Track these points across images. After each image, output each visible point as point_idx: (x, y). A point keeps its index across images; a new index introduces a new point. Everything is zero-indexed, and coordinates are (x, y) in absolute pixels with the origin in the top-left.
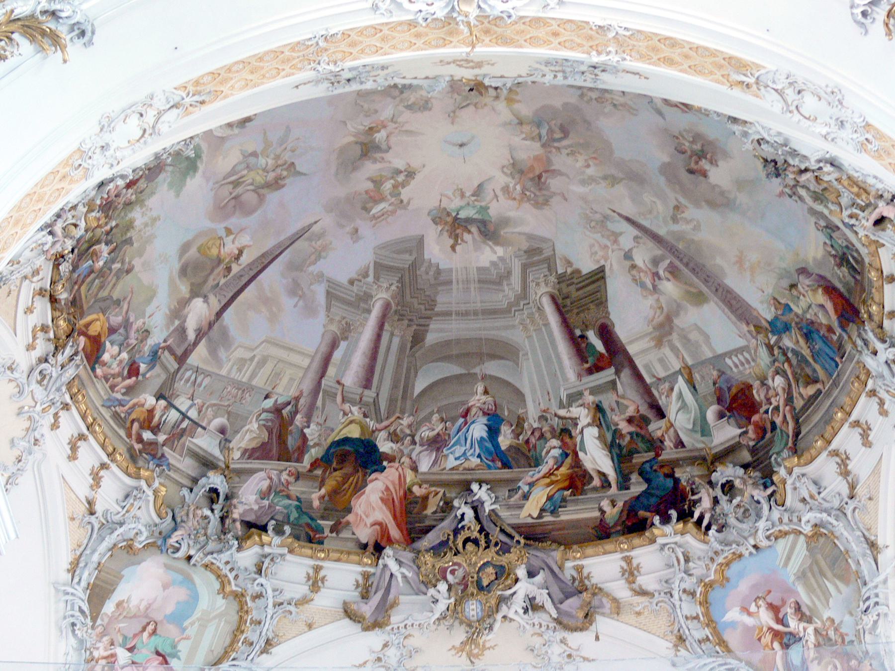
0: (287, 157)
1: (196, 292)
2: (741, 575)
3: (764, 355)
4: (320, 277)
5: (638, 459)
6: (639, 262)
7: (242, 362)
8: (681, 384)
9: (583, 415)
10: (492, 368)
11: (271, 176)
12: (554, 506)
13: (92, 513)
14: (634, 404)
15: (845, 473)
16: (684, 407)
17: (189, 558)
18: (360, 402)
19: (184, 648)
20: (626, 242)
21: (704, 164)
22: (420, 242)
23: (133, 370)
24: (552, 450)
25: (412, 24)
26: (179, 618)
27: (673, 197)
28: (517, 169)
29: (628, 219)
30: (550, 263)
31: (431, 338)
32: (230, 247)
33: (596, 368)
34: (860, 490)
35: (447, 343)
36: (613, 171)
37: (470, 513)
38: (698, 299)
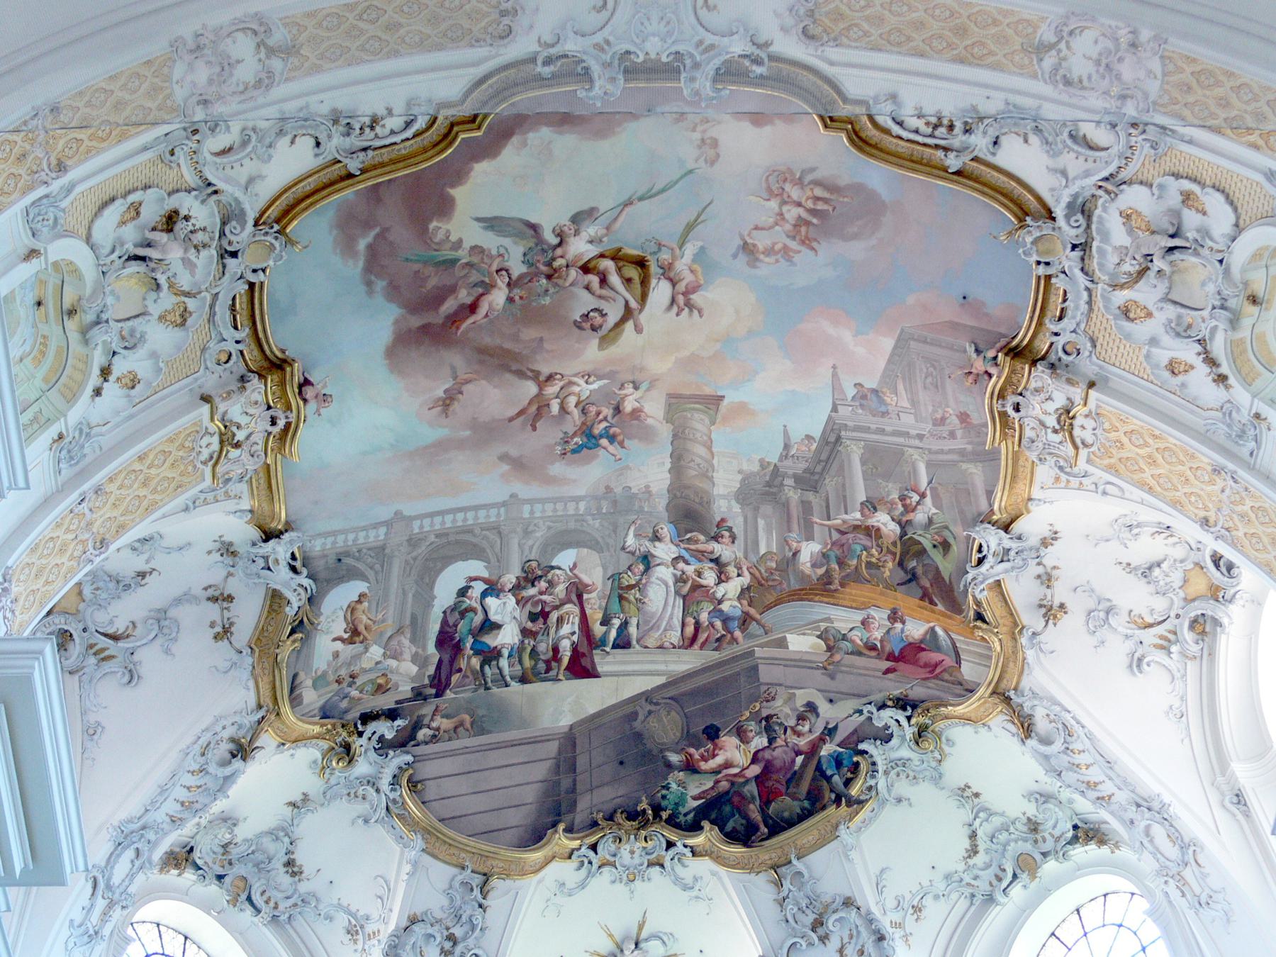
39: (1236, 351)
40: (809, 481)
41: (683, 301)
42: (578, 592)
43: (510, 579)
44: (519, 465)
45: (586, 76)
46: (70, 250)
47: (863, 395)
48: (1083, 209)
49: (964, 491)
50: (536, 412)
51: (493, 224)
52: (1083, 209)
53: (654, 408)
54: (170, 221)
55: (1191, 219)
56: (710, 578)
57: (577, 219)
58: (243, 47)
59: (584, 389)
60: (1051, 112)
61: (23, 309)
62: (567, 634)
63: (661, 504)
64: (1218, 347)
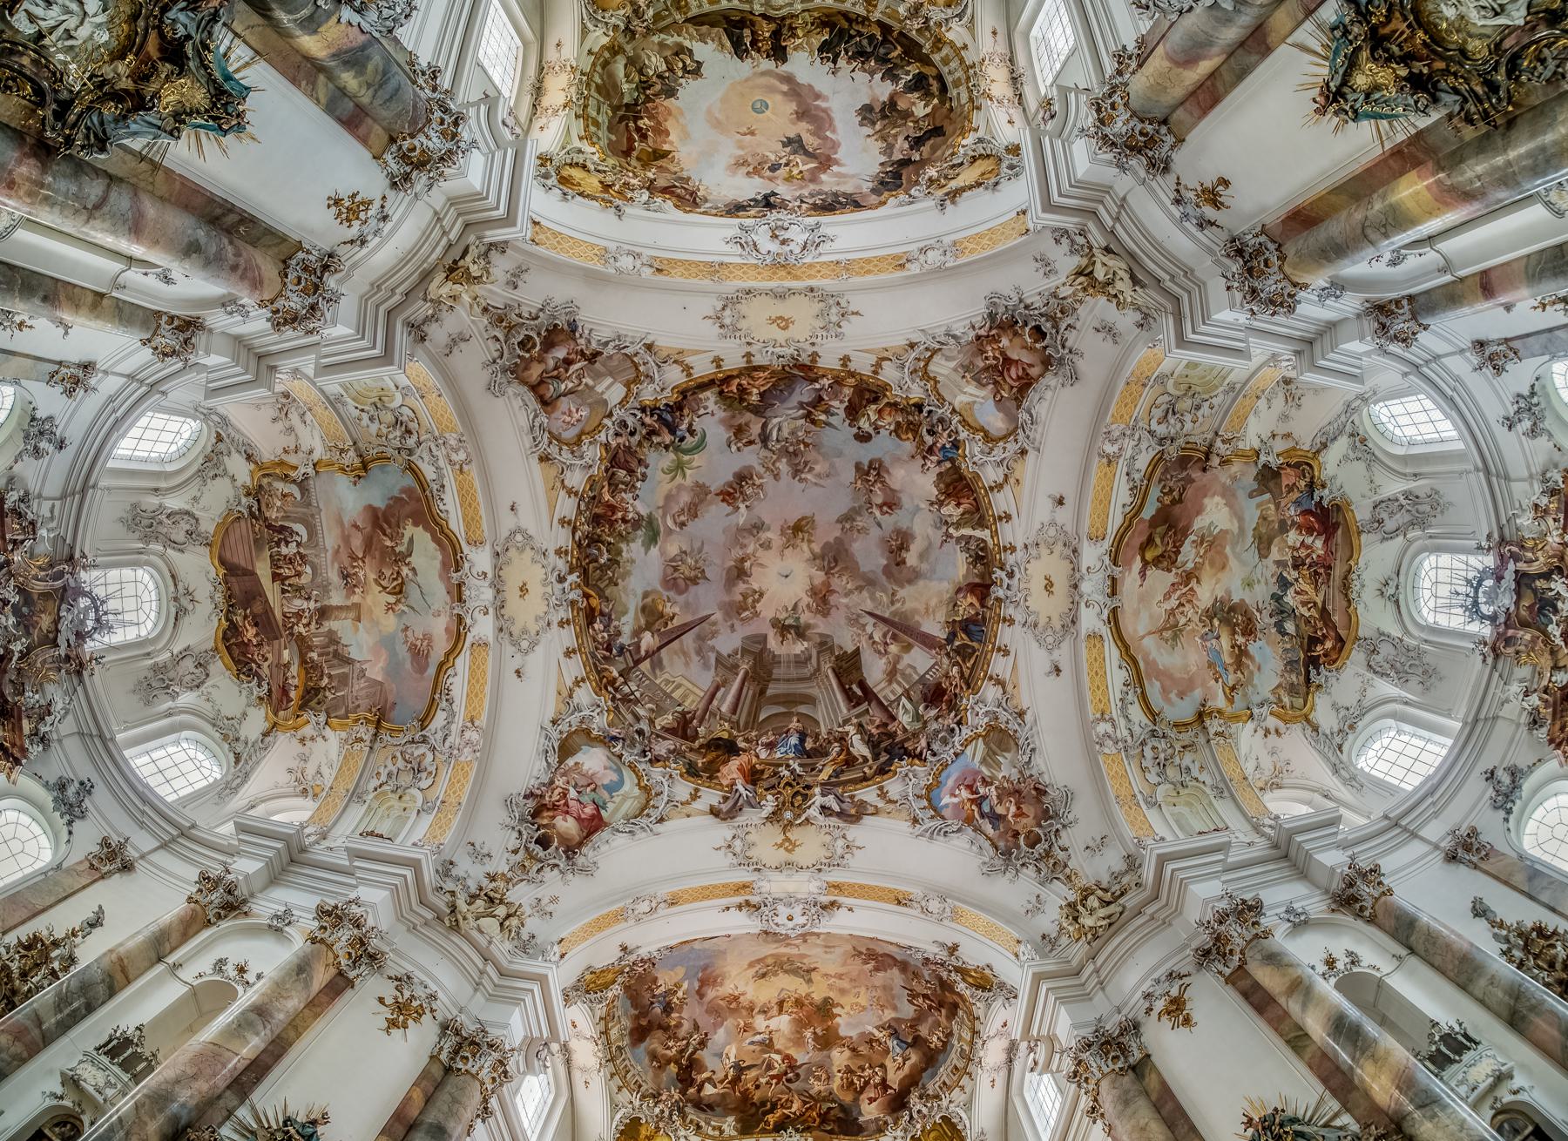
0: (701, 563)
1: (649, 627)
2: (948, 777)
3: (946, 661)
4: (713, 649)
5: (883, 745)
6: (877, 639)
7: (668, 682)
8: (904, 700)
9: (851, 729)
10: (802, 709)
11: (693, 574)
12: (837, 774)
13: (571, 696)
14: (878, 716)
15: (1000, 682)
16: (906, 711)
17: (620, 757)
18: (729, 721)
19: (610, 806)
20: (869, 629)
21: (904, 554)
22: (765, 637)
23: (609, 649)
24: (836, 748)
25: (756, 266)
26: (612, 788)
27: (890, 587)
28: (813, 592)
29: (870, 614)
30: (831, 649)
31: (769, 692)
32: (668, 610)
33: (858, 704)
34: (1009, 688)
35: (776, 696)
36: (862, 583)
37: (787, 773)
38: (907, 648)
39: (384, 793)
40: (336, 654)
41: (390, 607)
42: (299, 574)
43: (302, 550)
44: (337, 552)
45: (457, 571)
46: (398, 400)
47: (363, 671)
48: (424, 740)
49: (336, 708)
50: (353, 558)
51: (411, 540)
52: (424, 740)
53: (356, 599)
54: (409, 432)
55: (424, 775)
56: (304, 621)
57: (413, 569)
58: (462, 456)
59: (361, 574)
60: (453, 727)
61: (380, 384)
62: (286, 572)
63: (326, 603)
64: (385, 788)
